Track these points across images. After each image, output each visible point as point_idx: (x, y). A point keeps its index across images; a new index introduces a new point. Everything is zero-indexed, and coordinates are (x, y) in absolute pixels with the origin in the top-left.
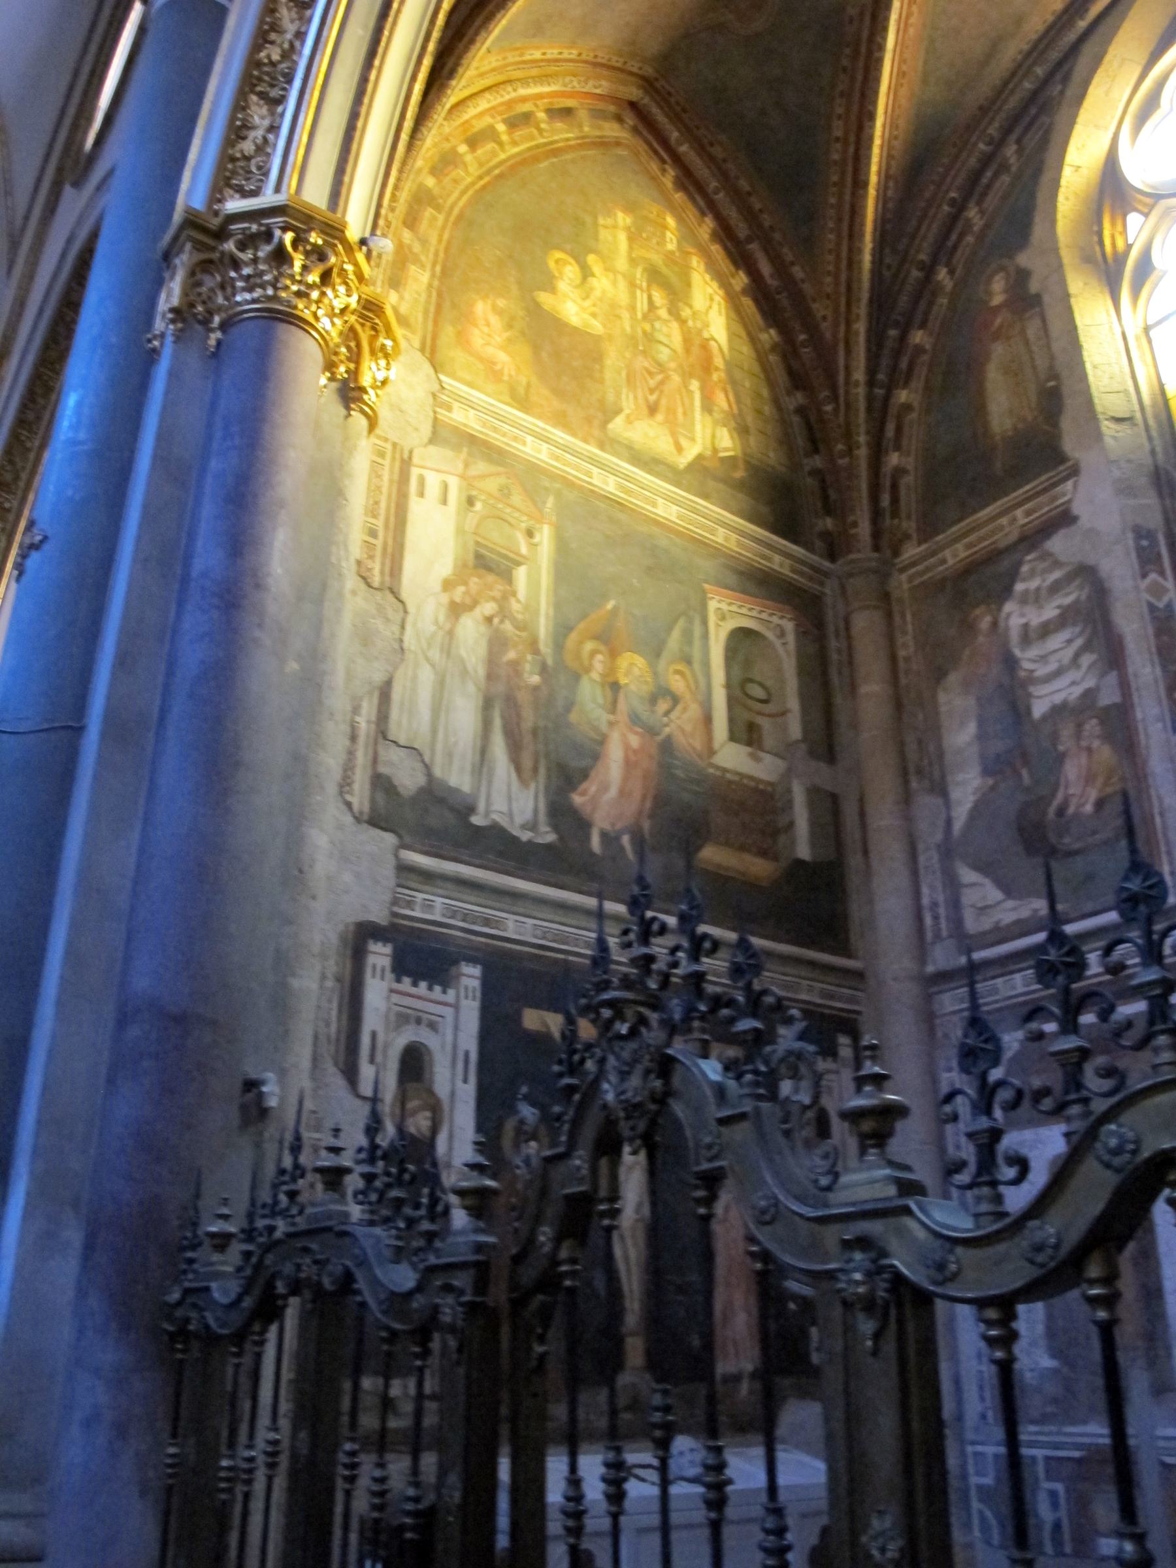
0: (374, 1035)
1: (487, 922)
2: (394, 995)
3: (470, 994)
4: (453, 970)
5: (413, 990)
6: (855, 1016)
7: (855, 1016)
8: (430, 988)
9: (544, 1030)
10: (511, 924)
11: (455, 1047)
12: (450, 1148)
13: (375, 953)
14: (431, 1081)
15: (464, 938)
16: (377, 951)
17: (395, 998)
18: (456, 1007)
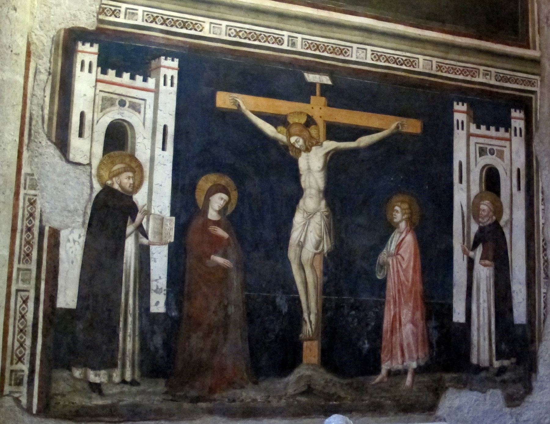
0: (82, 115)
1: (184, 25)
2: (99, 84)
3: (169, 82)
4: (154, 63)
5: (118, 80)
6: (530, 95)
7: (530, 95)
8: (132, 78)
9: (236, 108)
10: (207, 26)
11: (155, 122)
12: (150, 200)
13: (83, 52)
14: (133, 149)
15: (163, 38)
16: (85, 50)
17: (101, 86)
18: (156, 92)
